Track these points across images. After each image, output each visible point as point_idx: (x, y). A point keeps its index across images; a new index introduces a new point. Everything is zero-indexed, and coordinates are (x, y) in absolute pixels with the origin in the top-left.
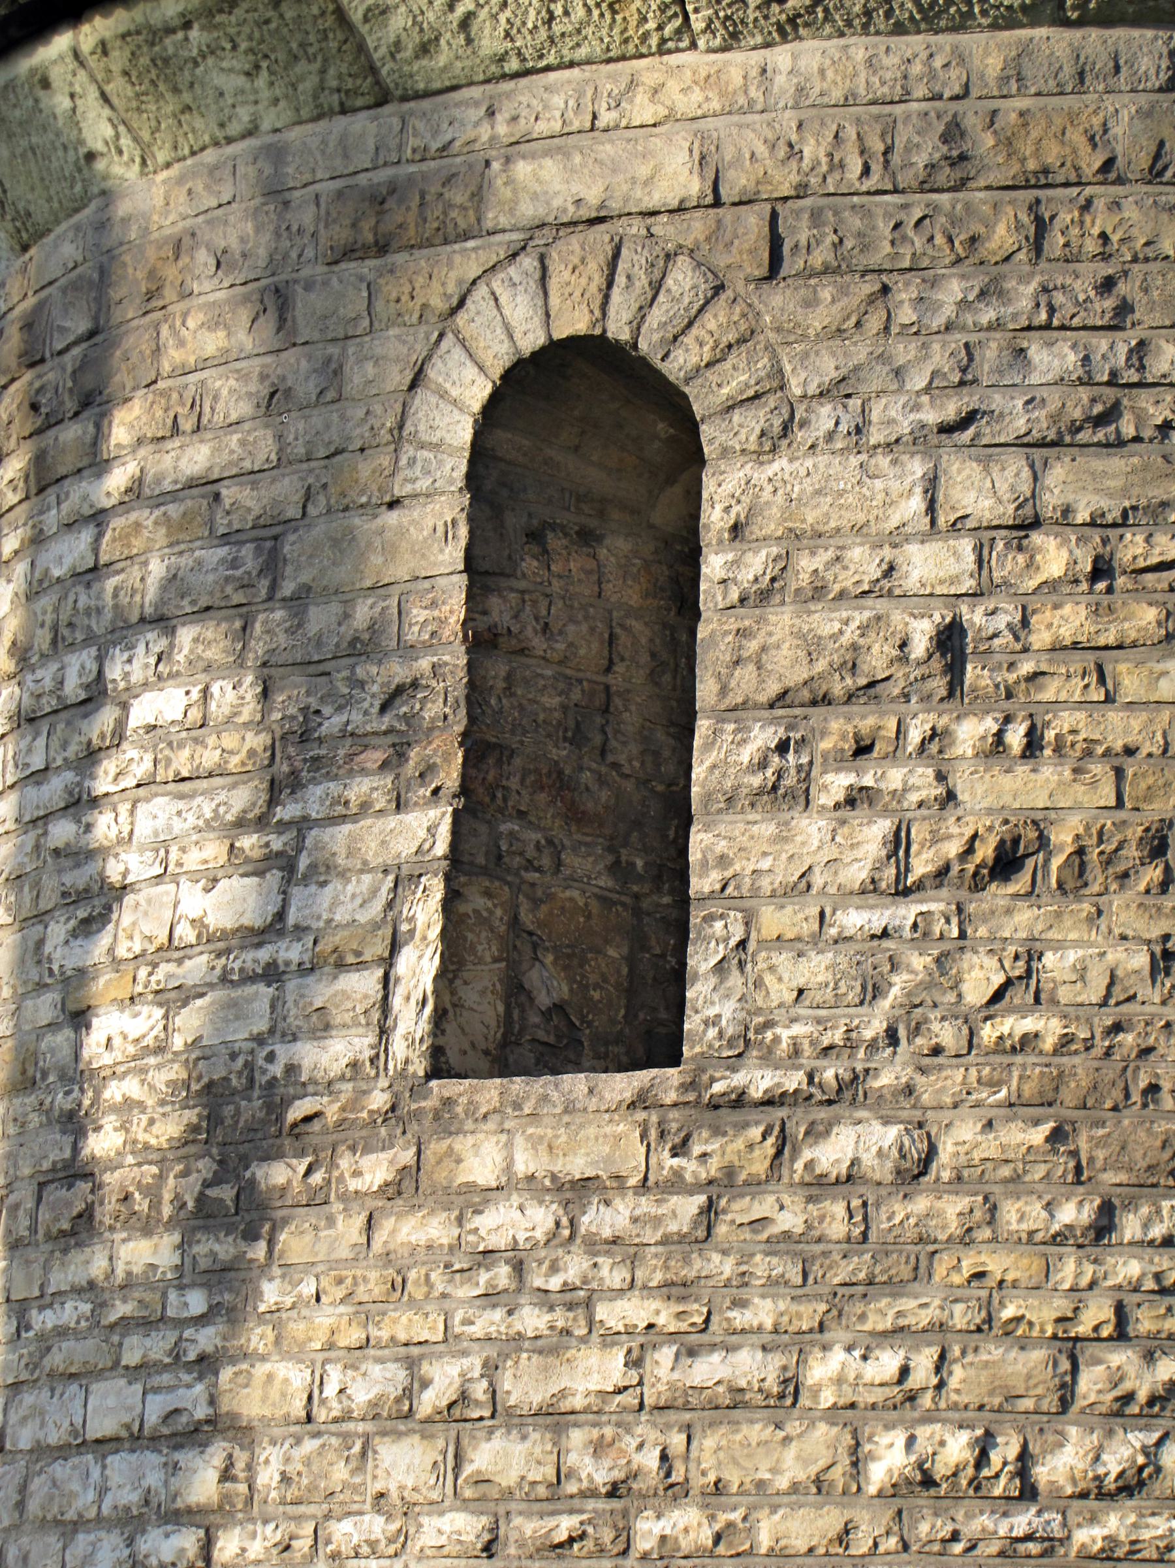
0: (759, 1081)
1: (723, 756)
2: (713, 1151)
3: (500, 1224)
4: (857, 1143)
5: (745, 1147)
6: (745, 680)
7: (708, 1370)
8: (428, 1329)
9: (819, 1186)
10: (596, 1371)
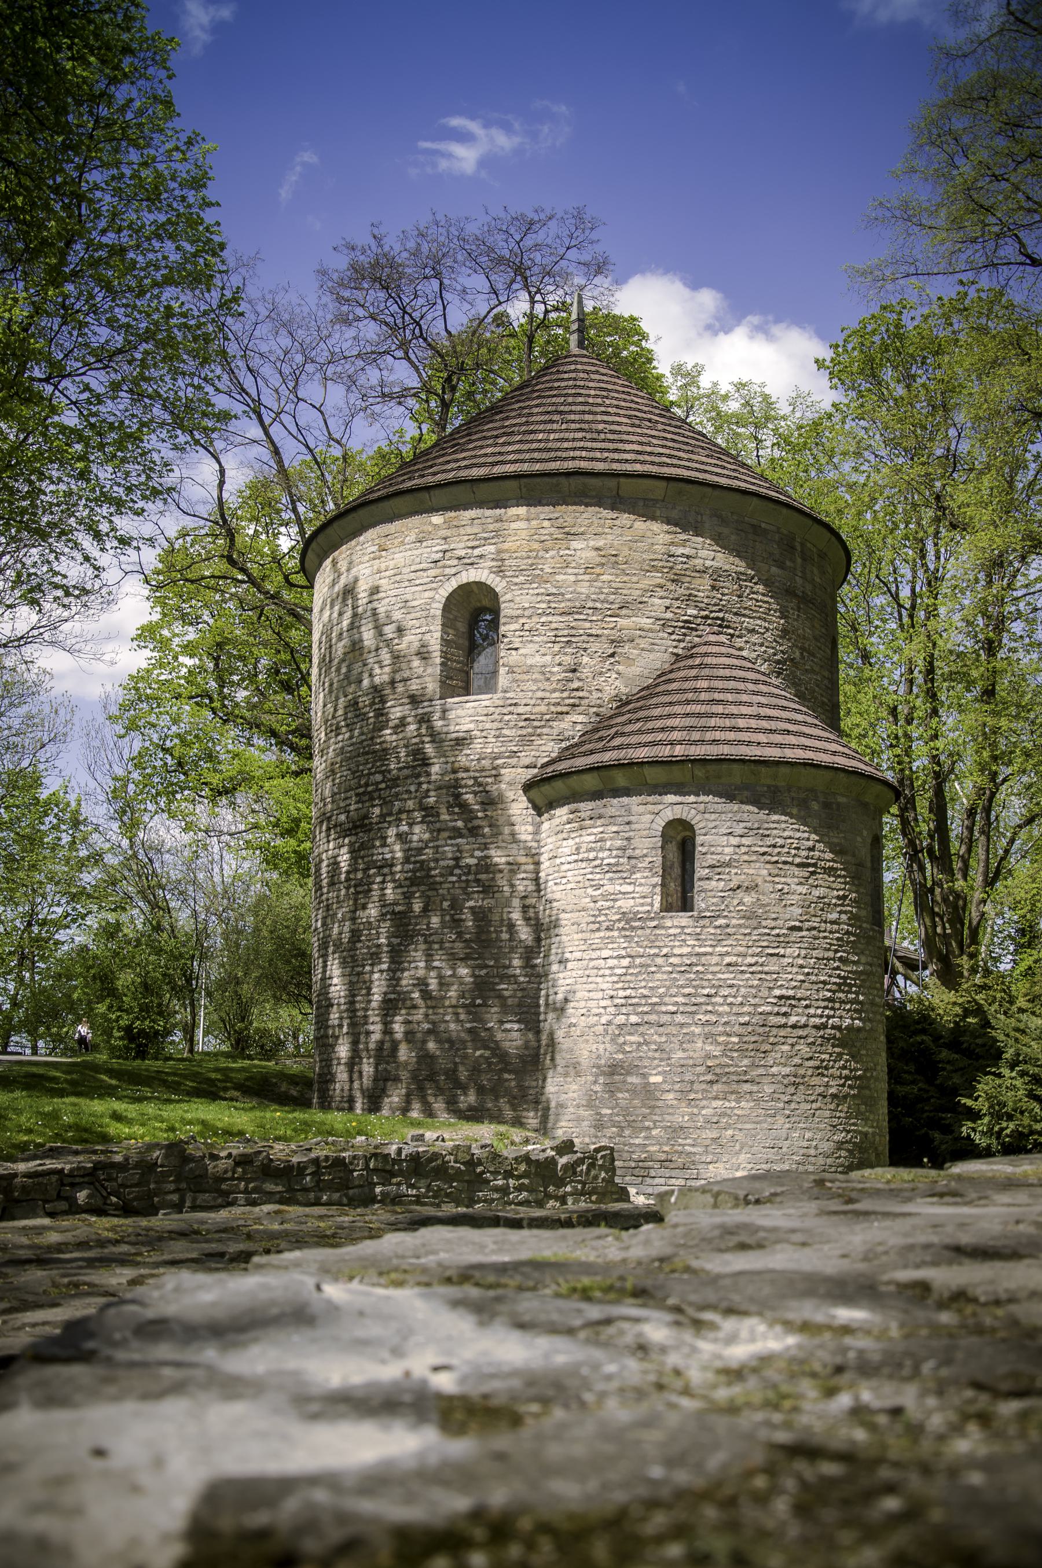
0: (708, 914)
1: (700, 872)
2: (702, 922)
3: (672, 931)
4: (721, 922)
5: (706, 922)
6: (704, 864)
7: (702, 950)
8: (662, 944)
9: (716, 927)
10: (685, 950)
